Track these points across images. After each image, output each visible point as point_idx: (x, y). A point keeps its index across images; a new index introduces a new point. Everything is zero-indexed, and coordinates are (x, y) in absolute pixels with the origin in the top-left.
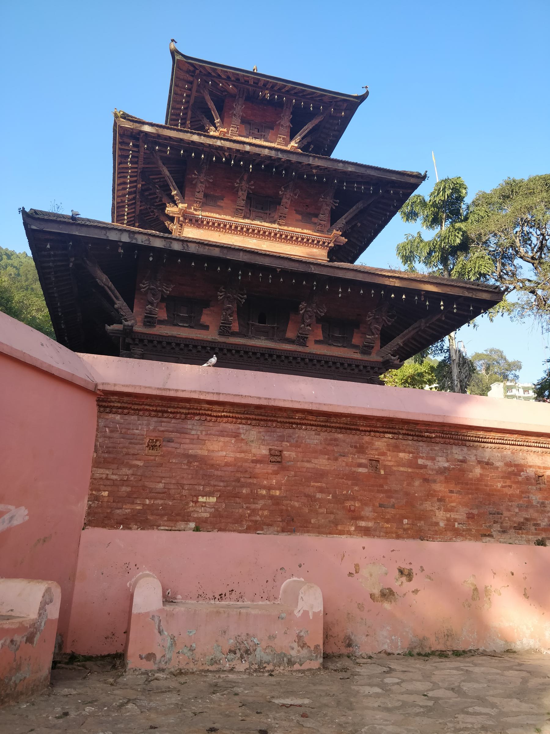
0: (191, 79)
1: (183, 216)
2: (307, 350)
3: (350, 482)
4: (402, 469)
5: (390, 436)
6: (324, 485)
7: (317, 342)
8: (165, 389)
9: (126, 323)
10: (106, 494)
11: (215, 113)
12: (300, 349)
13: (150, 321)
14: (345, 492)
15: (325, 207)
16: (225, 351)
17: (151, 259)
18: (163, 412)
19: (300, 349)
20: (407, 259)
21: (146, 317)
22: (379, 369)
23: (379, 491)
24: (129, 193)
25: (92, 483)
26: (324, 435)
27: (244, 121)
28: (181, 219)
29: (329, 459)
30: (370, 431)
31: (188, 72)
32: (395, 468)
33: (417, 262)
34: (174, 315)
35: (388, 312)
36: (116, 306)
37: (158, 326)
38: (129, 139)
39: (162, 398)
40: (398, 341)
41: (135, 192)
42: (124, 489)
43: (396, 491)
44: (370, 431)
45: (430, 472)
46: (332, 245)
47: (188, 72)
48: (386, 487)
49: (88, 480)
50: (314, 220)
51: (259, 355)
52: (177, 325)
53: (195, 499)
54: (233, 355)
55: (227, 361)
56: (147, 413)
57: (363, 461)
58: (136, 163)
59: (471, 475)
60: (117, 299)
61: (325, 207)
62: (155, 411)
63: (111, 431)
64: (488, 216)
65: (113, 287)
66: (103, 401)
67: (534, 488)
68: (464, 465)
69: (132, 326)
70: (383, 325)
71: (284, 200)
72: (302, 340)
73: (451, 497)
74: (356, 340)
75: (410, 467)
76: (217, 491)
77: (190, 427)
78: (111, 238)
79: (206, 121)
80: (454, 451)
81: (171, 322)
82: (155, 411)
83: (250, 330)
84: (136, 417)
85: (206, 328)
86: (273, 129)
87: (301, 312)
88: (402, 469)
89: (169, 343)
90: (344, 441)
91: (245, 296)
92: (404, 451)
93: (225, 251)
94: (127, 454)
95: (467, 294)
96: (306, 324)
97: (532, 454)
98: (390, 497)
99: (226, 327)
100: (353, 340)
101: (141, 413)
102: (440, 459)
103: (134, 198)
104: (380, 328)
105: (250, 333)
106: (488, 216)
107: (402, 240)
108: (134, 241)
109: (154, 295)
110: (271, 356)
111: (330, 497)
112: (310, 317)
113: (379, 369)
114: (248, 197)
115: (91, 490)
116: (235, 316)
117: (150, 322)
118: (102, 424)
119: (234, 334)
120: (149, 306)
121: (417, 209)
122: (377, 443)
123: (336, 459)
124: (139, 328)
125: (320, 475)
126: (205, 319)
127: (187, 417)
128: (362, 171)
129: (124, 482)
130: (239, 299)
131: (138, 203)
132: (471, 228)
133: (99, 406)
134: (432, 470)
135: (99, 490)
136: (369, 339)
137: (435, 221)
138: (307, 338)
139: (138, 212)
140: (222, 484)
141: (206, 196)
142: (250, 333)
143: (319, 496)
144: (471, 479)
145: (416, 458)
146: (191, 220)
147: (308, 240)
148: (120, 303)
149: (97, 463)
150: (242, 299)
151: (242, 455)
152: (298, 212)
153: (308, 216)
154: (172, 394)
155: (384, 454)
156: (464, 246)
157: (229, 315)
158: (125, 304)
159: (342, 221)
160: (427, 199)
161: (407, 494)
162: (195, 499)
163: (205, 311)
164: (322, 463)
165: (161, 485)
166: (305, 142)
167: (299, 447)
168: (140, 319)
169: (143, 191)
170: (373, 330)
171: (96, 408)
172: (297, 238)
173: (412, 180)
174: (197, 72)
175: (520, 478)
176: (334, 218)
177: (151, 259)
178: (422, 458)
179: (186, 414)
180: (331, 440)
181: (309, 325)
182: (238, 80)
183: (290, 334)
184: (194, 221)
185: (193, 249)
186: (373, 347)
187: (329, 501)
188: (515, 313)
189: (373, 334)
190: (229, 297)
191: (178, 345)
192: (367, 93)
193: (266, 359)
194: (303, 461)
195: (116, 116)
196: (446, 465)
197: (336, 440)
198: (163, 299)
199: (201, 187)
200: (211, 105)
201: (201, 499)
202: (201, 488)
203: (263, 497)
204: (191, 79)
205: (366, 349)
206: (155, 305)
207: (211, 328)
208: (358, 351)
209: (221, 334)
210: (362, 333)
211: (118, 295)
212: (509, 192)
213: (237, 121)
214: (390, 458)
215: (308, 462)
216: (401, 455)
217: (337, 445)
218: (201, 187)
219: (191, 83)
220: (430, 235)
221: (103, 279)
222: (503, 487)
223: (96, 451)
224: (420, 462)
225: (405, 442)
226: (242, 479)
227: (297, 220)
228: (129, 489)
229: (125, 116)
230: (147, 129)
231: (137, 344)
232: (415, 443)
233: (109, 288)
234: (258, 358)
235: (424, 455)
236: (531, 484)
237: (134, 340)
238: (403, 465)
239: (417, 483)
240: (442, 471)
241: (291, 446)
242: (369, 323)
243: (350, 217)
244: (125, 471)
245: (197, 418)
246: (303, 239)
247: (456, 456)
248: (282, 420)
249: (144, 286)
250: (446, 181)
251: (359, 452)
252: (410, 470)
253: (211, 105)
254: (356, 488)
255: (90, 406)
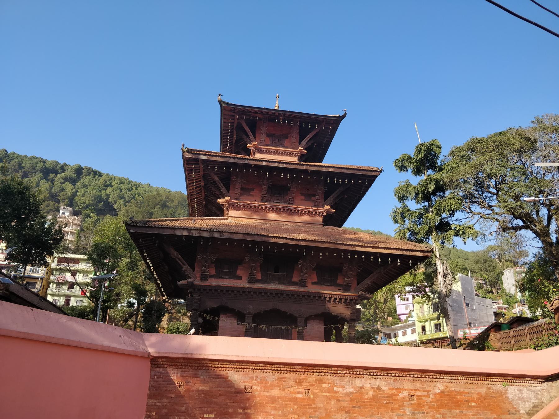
0: (234, 114)
1: (228, 203)
2: (306, 290)
3: (292, 403)
4: (324, 394)
5: (317, 374)
6: (276, 405)
7: (313, 283)
8: (185, 354)
9: (189, 280)
10: (154, 414)
11: (250, 133)
12: (301, 289)
13: (204, 277)
14: (289, 409)
15: (319, 191)
16: (252, 293)
17: (202, 243)
18: (185, 366)
19: (301, 289)
20: (402, 198)
21: (202, 274)
23: (309, 408)
24: (196, 188)
25: (147, 408)
26: (277, 375)
27: (268, 135)
28: (227, 205)
29: (280, 390)
30: (305, 372)
31: (231, 111)
32: (319, 394)
33: (410, 200)
36: (183, 269)
37: (209, 280)
38: (193, 163)
39: (184, 359)
40: (368, 282)
41: (200, 186)
42: (164, 410)
43: (319, 408)
44: (305, 372)
45: (341, 395)
46: (325, 214)
47: (231, 111)
48: (314, 406)
49: (145, 406)
50: (313, 198)
51: (274, 295)
52: (222, 278)
53: (202, 416)
56: (177, 367)
57: (301, 390)
58: (199, 172)
59: (366, 396)
60: (184, 265)
61: (319, 191)
62: (181, 365)
63: (158, 378)
64: (458, 166)
65: (181, 258)
66: (153, 361)
67: (408, 403)
68: (363, 390)
69: (193, 282)
71: (292, 189)
72: (303, 283)
73: (354, 410)
74: (339, 281)
75: (329, 392)
76: (215, 411)
77: (200, 374)
78: (177, 234)
79: (244, 137)
80: (357, 381)
81: (218, 276)
82: (181, 365)
84: (171, 369)
85: (240, 278)
86: (287, 138)
88: (324, 394)
89: (216, 290)
90: (289, 378)
92: (326, 383)
93: (246, 236)
94: (166, 391)
95: (405, 253)
97: (407, 381)
98: (315, 412)
100: (338, 281)
101: (173, 367)
102: (348, 387)
103: (200, 189)
106: (458, 166)
107: (397, 185)
108: (191, 235)
109: (206, 261)
110: (282, 294)
111: (280, 413)
113: (356, 300)
114: (269, 187)
115: (147, 412)
116: (259, 269)
118: (153, 374)
119: (258, 281)
121: (406, 164)
122: (309, 379)
123: (284, 390)
124: (198, 282)
125: (274, 399)
126: (239, 272)
127: (198, 368)
128: (339, 170)
129: (164, 407)
131: (203, 192)
132: (444, 176)
133: (152, 364)
134: (342, 394)
135: (150, 412)
137: (418, 171)
139: (203, 196)
140: (217, 407)
141: (242, 189)
143: (273, 412)
144: (367, 399)
145: (333, 387)
146: (233, 206)
147: (309, 212)
148: (186, 268)
149: (150, 397)
151: (229, 389)
152: (302, 194)
153: (309, 196)
154: (189, 356)
155: (313, 385)
156: (440, 188)
158: (189, 267)
159: (331, 199)
160: (412, 156)
161: (326, 409)
162: (202, 416)
163: (240, 267)
164: (275, 392)
165: (184, 408)
166: (309, 144)
167: (263, 383)
168: (198, 275)
169: (205, 185)
171: (150, 365)
172: (302, 211)
173: (373, 174)
174: (236, 111)
175: (398, 397)
176: (326, 198)
177: (202, 243)
178: (337, 387)
179: (198, 367)
180: (282, 378)
181: (307, 274)
182: (262, 112)
183: (295, 279)
184: (235, 206)
185: (226, 236)
186: (351, 286)
187: (279, 415)
188: (479, 238)
189: (349, 278)
191: (222, 291)
192: (345, 114)
193: (279, 297)
194: (264, 392)
195: (183, 152)
196: (351, 390)
197: (284, 378)
198: (212, 262)
199: (238, 185)
200: (247, 129)
201: (205, 416)
202: (206, 409)
203: (241, 414)
204: (234, 114)
205: (346, 288)
209: (250, 282)
211: (184, 262)
212: (474, 146)
213: (263, 136)
214: (316, 388)
215: (268, 392)
216: (324, 385)
217: (285, 381)
218: (238, 185)
219: (234, 116)
220: (416, 181)
221: (174, 254)
222: (387, 403)
223: (149, 389)
224: (335, 389)
225: (326, 377)
226: (229, 404)
227: (302, 200)
228: (166, 411)
229: (189, 151)
230: (203, 157)
232: (332, 377)
235: (338, 385)
236: (406, 401)
237: (194, 289)
238: (325, 392)
239: (333, 402)
240: (348, 395)
241: (258, 383)
243: (336, 196)
244: (165, 400)
245: (204, 368)
246: (305, 212)
247: (358, 385)
248: (252, 367)
249: (199, 257)
250: (422, 145)
251: (297, 385)
252: (328, 394)
253: (247, 129)
254: (296, 407)
255: (148, 364)
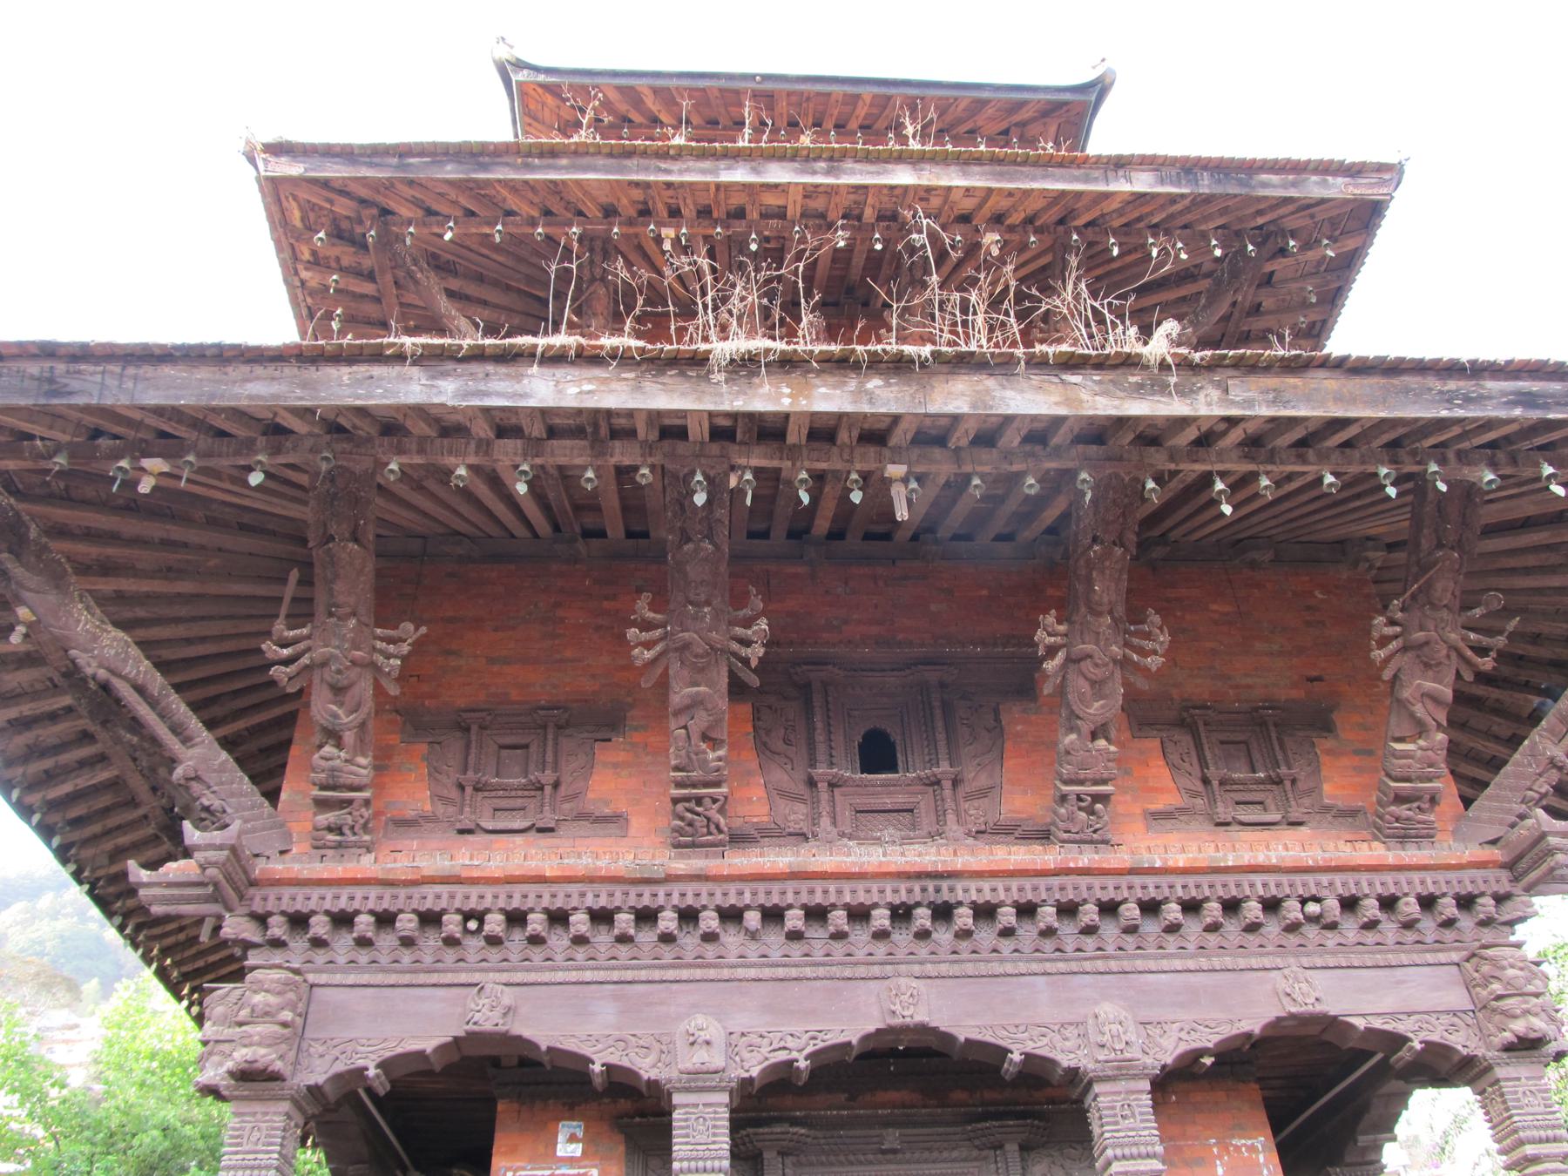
16: (710, 921)
22: (1500, 899)
34: (462, 788)
35: (1466, 607)
36: (179, 772)
54: (753, 935)
55: (726, 973)
60: (187, 740)
70: (1458, 675)
83: (825, 807)
87: (1050, 666)
91: (763, 624)
96: (1086, 728)
99: (699, 800)
100: (1326, 787)
104: (1448, 693)
105: (825, 821)
112: (1097, 685)
117: (338, 830)
120: (328, 750)
130: (735, 646)
136: (1406, 755)
138: (1103, 798)
142: (825, 821)
150: (746, 643)
157: (705, 737)
170: (1419, 710)
190: (686, 646)
206: (349, 737)
207: (635, 823)
208: (1365, 834)
209: (684, 842)
210: (1356, 752)
231: (277, 944)
233: (140, 690)
234: (881, 935)
237: (262, 919)
242: (1387, 675)
